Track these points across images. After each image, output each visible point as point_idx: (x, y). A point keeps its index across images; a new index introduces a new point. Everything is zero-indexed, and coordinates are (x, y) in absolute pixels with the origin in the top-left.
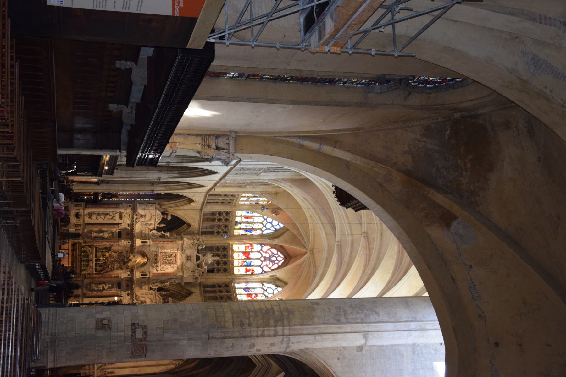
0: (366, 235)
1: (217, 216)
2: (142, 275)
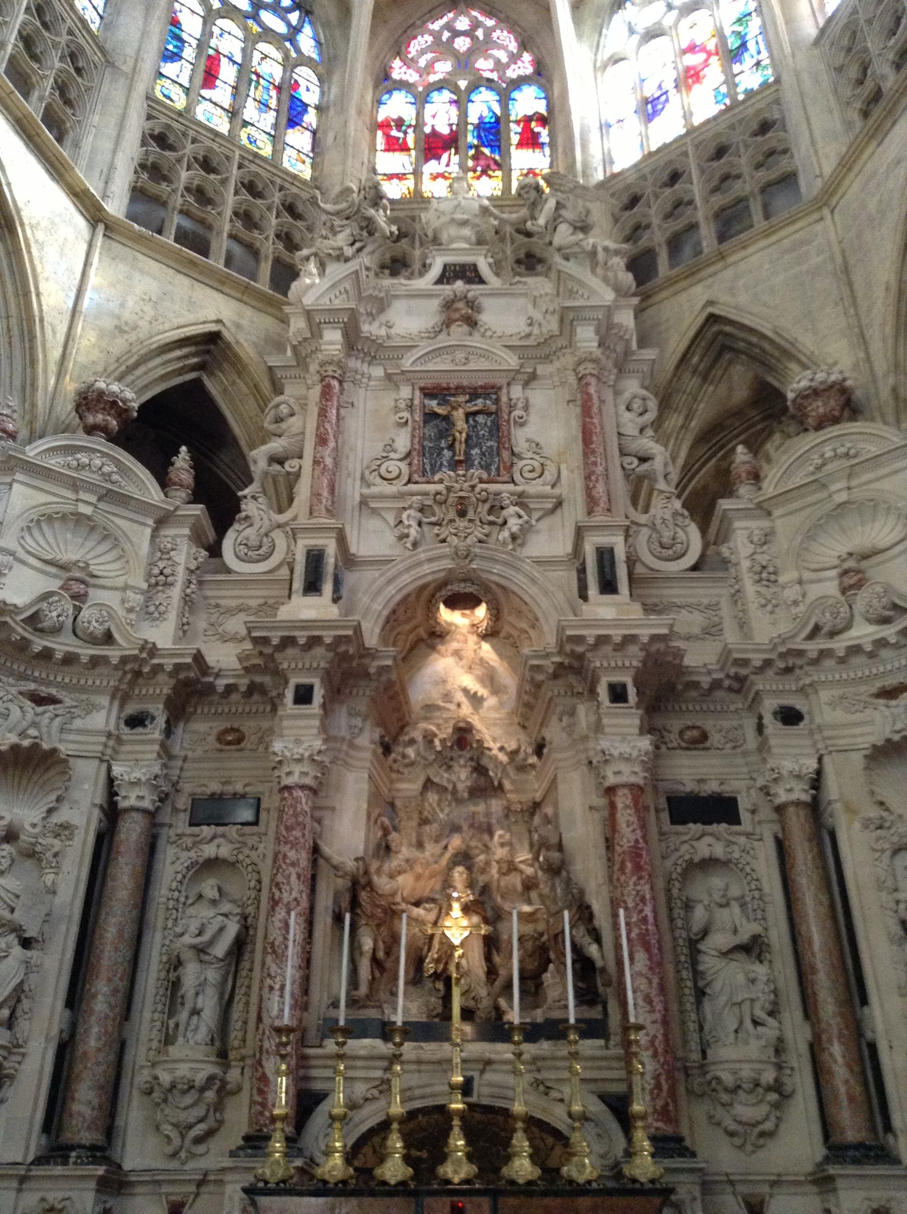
2: (608, 586)
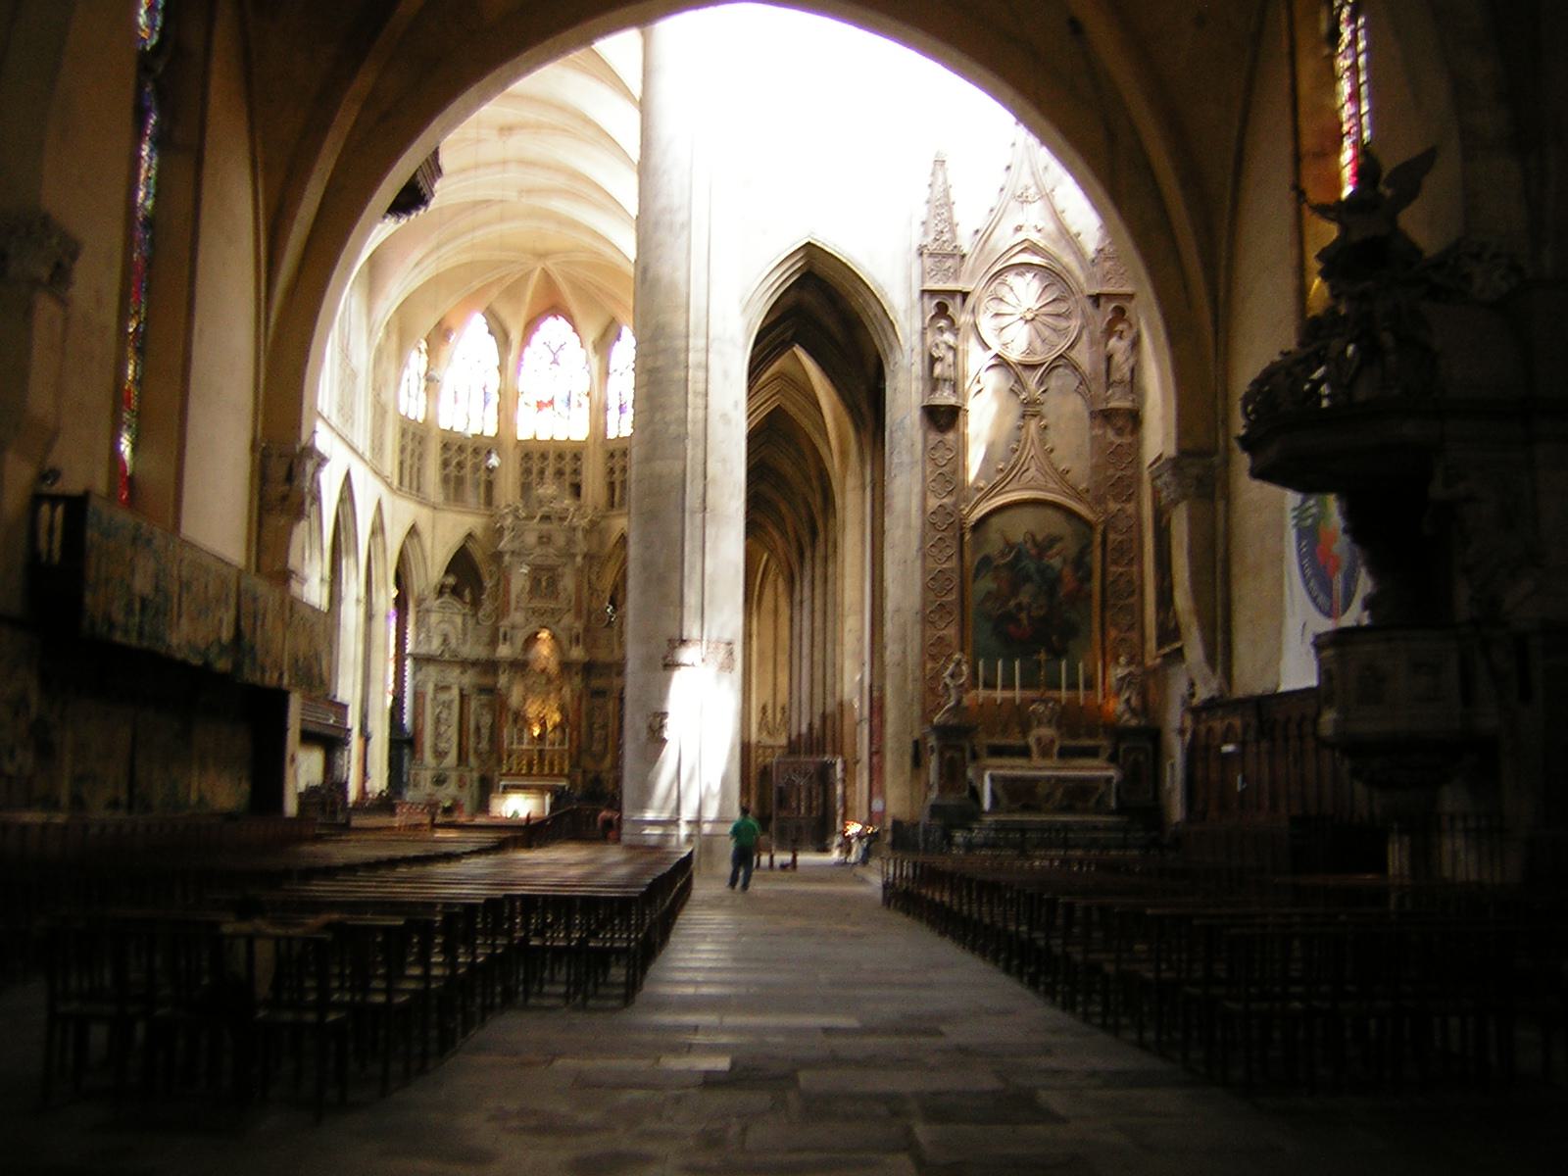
0: (506, 130)
1: (452, 470)
